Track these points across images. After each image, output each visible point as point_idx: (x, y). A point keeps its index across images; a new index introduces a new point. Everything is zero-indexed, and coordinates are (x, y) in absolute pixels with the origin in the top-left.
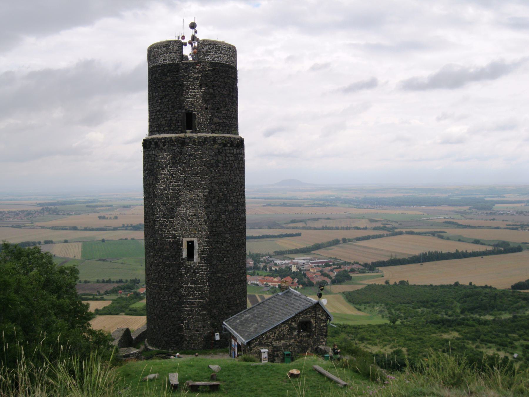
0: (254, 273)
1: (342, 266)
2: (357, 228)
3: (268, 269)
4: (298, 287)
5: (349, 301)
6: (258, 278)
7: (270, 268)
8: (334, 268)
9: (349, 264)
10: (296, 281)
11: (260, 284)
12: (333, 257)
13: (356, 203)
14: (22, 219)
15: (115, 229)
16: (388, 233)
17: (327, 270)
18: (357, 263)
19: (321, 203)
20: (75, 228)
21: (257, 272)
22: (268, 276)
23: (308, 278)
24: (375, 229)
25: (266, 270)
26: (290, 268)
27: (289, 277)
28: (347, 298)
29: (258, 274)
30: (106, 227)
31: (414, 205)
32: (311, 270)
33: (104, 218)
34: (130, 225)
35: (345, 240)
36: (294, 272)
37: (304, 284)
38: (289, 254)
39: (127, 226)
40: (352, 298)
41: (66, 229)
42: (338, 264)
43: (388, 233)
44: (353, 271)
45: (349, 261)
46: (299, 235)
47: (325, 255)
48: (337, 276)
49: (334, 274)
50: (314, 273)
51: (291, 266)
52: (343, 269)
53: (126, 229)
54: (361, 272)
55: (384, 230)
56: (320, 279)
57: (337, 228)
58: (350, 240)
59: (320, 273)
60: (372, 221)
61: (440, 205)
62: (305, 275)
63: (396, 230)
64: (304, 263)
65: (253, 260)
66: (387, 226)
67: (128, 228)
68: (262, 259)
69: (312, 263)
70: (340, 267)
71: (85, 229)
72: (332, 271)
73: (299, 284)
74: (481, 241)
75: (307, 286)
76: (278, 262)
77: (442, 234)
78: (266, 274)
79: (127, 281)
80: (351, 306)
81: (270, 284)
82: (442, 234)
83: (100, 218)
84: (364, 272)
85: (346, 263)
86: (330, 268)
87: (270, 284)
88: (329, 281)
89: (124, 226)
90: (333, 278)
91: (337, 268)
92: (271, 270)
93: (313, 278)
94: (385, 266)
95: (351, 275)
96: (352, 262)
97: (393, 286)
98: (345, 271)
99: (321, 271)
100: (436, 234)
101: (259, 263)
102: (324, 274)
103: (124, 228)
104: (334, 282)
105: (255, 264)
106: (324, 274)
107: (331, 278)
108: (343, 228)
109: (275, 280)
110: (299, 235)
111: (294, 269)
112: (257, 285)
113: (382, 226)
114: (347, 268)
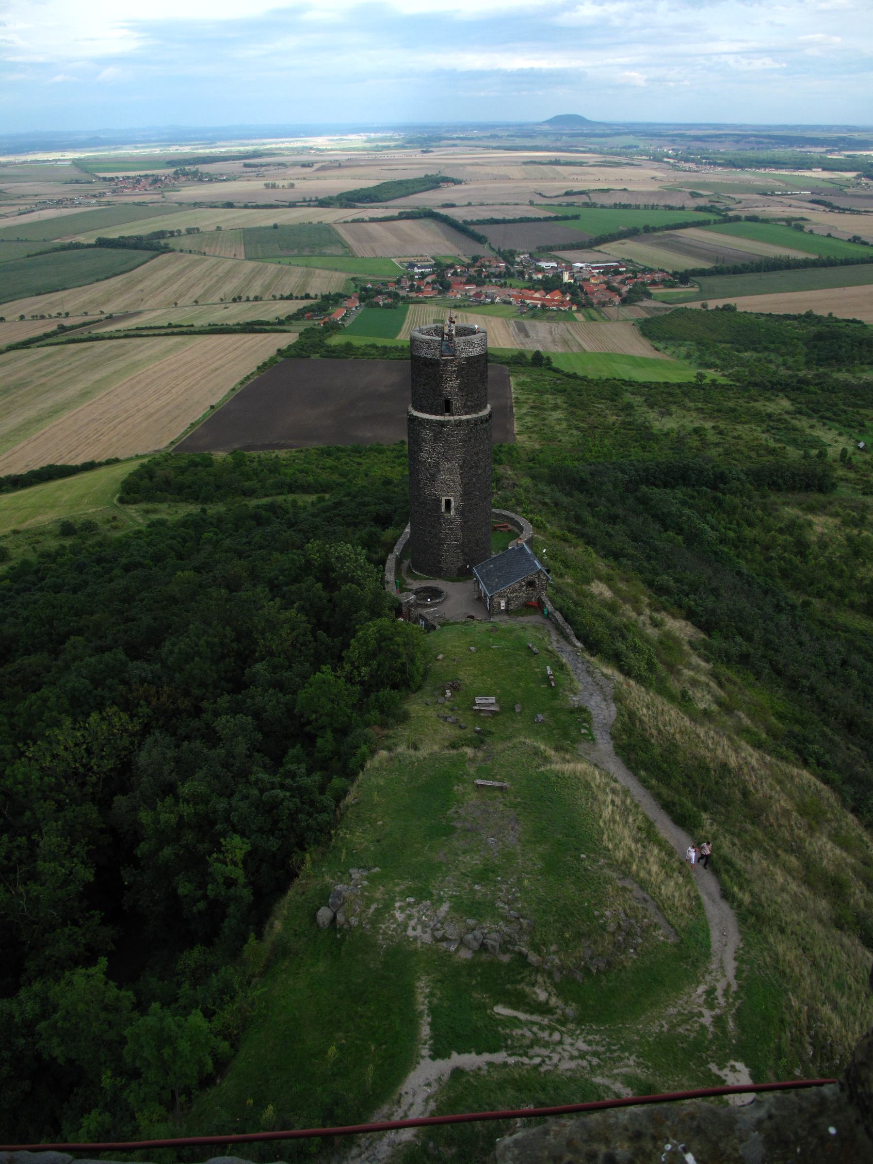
0: (505, 283)
1: (639, 275)
2: (671, 208)
3: (526, 276)
4: (570, 308)
5: (644, 335)
6: (514, 292)
7: (530, 275)
8: (627, 279)
9: (651, 271)
10: (568, 299)
11: (514, 302)
12: (627, 257)
13: (671, 161)
14: (146, 190)
15: (293, 205)
16: (717, 218)
17: (616, 281)
18: (662, 271)
19: (616, 159)
20: (230, 205)
21: (509, 281)
22: (525, 288)
23: (586, 294)
24: (699, 209)
25: (524, 278)
26: (559, 277)
27: (557, 291)
28: (642, 329)
29: (511, 285)
30: (277, 203)
31: (765, 167)
32: (592, 281)
33: (274, 186)
34: (314, 199)
35: (647, 229)
36: (566, 284)
37: (581, 306)
38: (559, 250)
39: (310, 201)
40: (649, 329)
41: (216, 207)
42: (634, 272)
43: (717, 218)
44: (654, 283)
45: (650, 266)
46: (576, 217)
47: (615, 251)
48: (630, 291)
49: (625, 289)
50: (596, 285)
51: (562, 272)
52: (639, 280)
53: (309, 206)
54: (666, 287)
55: (711, 211)
56: (605, 296)
57: (637, 207)
58: (655, 229)
59: (605, 286)
60: (694, 195)
61: (809, 169)
62: (581, 287)
63: (731, 214)
64: (581, 268)
65: (506, 260)
66: (717, 205)
67: (312, 203)
68: (518, 260)
69: (594, 268)
70: (636, 277)
71: (246, 207)
72: (623, 282)
73: (573, 304)
74: (863, 239)
75: (584, 306)
76: (543, 265)
77: (801, 223)
78: (522, 285)
79: (316, 297)
80: (646, 342)
81: (528, 301)
82: (801, 223)
83: (267, 186)
84: (672, 287)
85: (647, 270)
86: (620, 278)
87: (528, 301)
88: (617, 299)
89: (304, 201)
90: (625, 295)
91: (630, 278)
92: (531, 278)
93: (593, 293)
94: (704, 275)
95: (651, 291)
96: (655, 267)
97: (712, 310)
98: (644, 284)
99: (607, 283)
100: (793, 223)
101: (512, 265)
102: (610, 288)
103: (306, 204)
104: (625, 302)
105: (506, 267)
106: (610, 288)
107: (620, 295)
108: (646, 207)
109: (537, 295)
110: (576, 217)
111: (566, 278)
112: (510, 303)
113: (709, 205)
114: (647, 278)
